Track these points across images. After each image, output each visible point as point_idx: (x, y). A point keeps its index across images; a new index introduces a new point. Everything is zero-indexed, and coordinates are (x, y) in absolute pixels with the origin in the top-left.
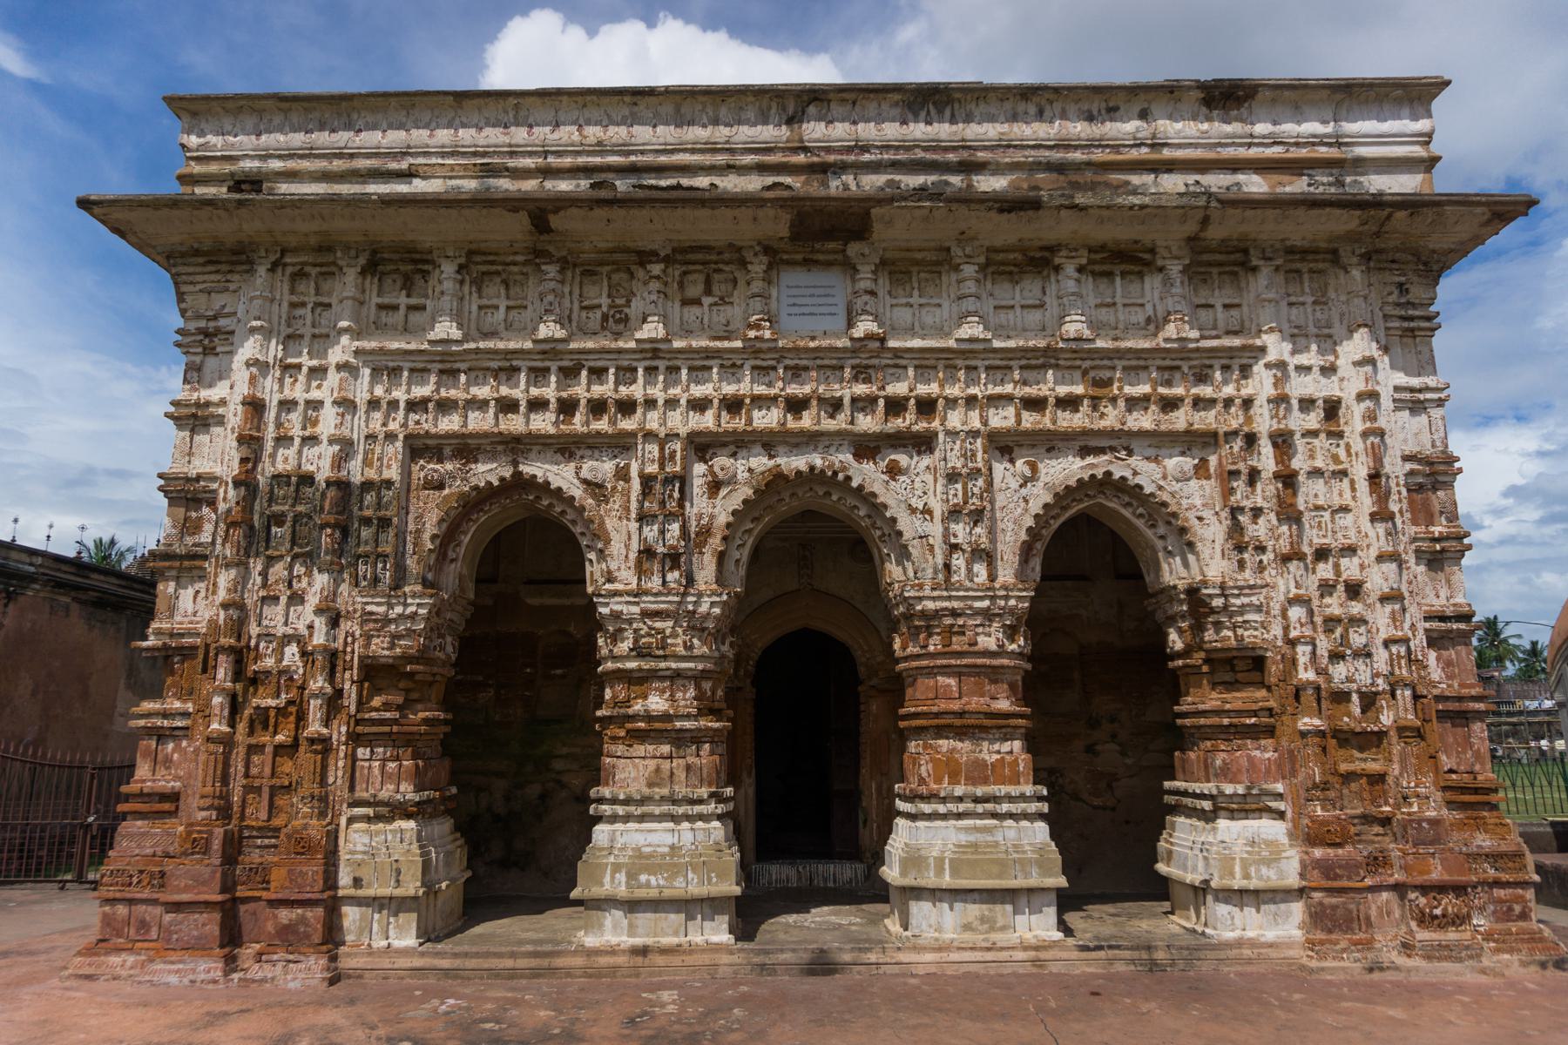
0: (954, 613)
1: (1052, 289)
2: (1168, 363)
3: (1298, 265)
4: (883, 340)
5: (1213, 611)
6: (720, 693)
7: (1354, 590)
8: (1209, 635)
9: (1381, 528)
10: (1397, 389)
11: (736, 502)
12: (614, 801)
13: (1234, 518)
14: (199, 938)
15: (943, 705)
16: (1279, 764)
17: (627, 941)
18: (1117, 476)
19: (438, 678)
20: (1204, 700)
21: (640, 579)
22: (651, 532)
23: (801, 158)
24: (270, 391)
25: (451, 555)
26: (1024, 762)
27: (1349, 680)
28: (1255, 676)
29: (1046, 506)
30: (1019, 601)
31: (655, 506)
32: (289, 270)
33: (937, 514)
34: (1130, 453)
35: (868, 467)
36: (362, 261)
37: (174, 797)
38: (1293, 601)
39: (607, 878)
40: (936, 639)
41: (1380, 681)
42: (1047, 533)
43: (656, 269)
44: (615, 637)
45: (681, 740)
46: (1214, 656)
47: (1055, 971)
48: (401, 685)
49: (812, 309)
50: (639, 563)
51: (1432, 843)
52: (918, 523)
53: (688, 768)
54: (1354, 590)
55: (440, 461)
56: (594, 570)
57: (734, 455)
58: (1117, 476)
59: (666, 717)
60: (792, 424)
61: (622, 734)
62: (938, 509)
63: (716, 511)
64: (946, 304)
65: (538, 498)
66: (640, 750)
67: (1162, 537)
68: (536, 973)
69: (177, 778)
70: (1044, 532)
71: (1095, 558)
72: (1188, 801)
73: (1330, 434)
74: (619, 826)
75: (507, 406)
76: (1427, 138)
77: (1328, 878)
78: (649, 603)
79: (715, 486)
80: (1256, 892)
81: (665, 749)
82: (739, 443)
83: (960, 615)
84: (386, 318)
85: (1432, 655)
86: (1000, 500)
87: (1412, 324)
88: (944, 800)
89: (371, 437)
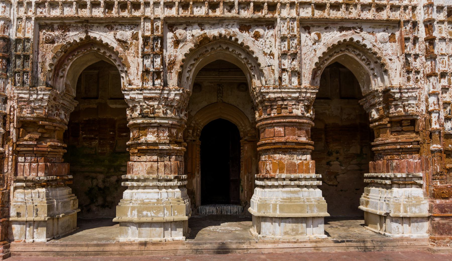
0: (283, 99)
5: (395, 100)
6: (180, 135)
8: (392, 110)
12: (132, 180)
13: (406, 59)
15: (277, 140)
16: (421, 165)
17: (138, 239)
18: (355, 40)
19: (57, 128)
20: (388, 138)
21: (143, 83)
22: (148, 62)
25: (61, 74)
26: (312, 163)
28: (411, 128)
29: (324, 53)
30: (311, 94)
31: (150, 50)
33: (276, 56)
34: (361, 30)
35: (245, 34)
38: (430, 95)
39: (129, 213)
40: (275, 111)
42: (323, 67)
44: (133, 109)
45: (162, 154)
46: (393, 120)
47: (324, 251)
48: (39, 130)
50: (143, 76)
52: (267, 60)
53: (165, 166)
55: (53, 31)
56: (124, 82)
57: (185, 29)
58: (355, 40)
59: (155, 144)
60: (211, 14)
61: (136, 151)
62: (276, 53)
63: (177, 54)
65: (99, 49)
66: (144, 158)
67: (372, 69)
68: (97, 253)
70: (322, 66)
71: (342, 79)
72: (379, 181)
74: (135, 191)
77: (442, 212)
78: (147, 94)
79: (177, 43)
80: (409, 218)
81: (155, 158)
82: (188, 23)
83: (285, 100)
86: (304, 50)
88: (277, 180)
89: (19, 19)
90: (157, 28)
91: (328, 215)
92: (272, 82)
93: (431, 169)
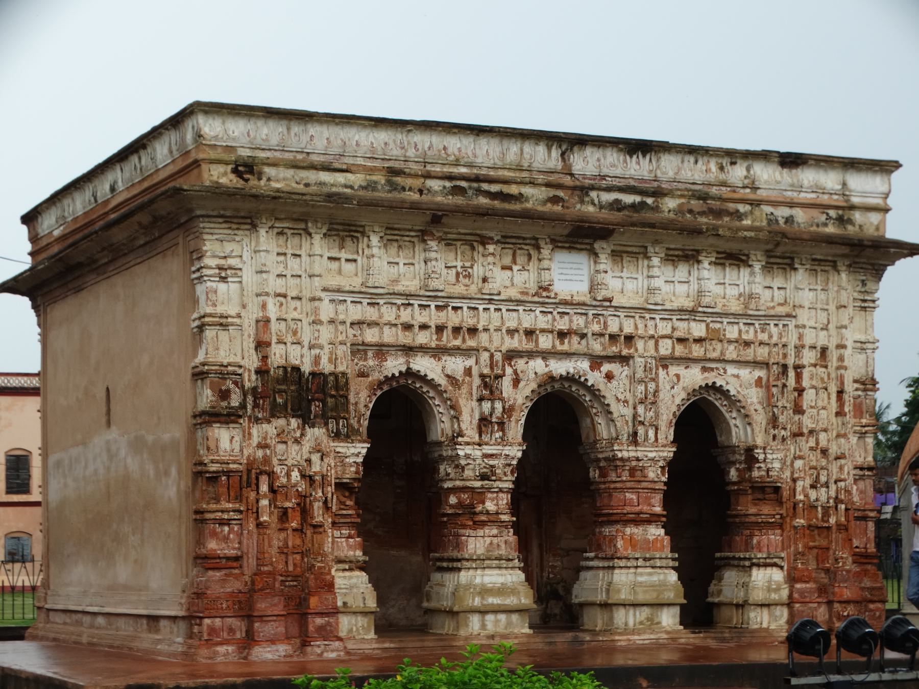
0: (638, 459)
1: (695, 273)
2: (749, 321)
3: (816, 267)
4: (611, 301)
7: (824, 452)
8: (756, 474)
9: (840, 419)
10: (855, 342)
11: (527, 392)
12: (468, 560)
14: (275, 634)
15: (628, 509)
18: (718, 385)
21: (480, 436)
22: (487, 406)
23: (567, 180)
24: (273, 312)
26: (667, 540)
27: (817, 500)
32: (276, 230)
33: (631, 403)
35: (596, 374)
36: (324, 231)
37: (237, 559)
41: (831, 501)
43: (491, 248)
49: (569, 275)
51: (846, 582)
52: (621, 408)
53: (506, 542)
54: (824, 452)
58: (718, 385)
60: (559, 347)
64: (640, 279)
66: (480, 532)
69: (234, 549)
73: (822, 366)
75: (408, 327)
76: (886, 195)
78: (488, 450)
79: (516, 382)
81: (495, 531)
82: (531, 355)
84: (334, 265)
85: (855, 487)
87: (866, 305)
90: (497, 362)
91: (685, 602)
92: (626, 435)
93: (792, 549)
